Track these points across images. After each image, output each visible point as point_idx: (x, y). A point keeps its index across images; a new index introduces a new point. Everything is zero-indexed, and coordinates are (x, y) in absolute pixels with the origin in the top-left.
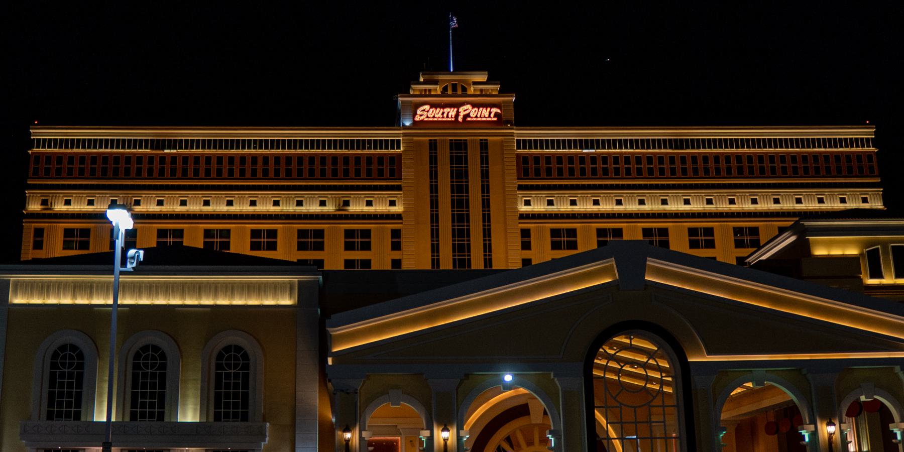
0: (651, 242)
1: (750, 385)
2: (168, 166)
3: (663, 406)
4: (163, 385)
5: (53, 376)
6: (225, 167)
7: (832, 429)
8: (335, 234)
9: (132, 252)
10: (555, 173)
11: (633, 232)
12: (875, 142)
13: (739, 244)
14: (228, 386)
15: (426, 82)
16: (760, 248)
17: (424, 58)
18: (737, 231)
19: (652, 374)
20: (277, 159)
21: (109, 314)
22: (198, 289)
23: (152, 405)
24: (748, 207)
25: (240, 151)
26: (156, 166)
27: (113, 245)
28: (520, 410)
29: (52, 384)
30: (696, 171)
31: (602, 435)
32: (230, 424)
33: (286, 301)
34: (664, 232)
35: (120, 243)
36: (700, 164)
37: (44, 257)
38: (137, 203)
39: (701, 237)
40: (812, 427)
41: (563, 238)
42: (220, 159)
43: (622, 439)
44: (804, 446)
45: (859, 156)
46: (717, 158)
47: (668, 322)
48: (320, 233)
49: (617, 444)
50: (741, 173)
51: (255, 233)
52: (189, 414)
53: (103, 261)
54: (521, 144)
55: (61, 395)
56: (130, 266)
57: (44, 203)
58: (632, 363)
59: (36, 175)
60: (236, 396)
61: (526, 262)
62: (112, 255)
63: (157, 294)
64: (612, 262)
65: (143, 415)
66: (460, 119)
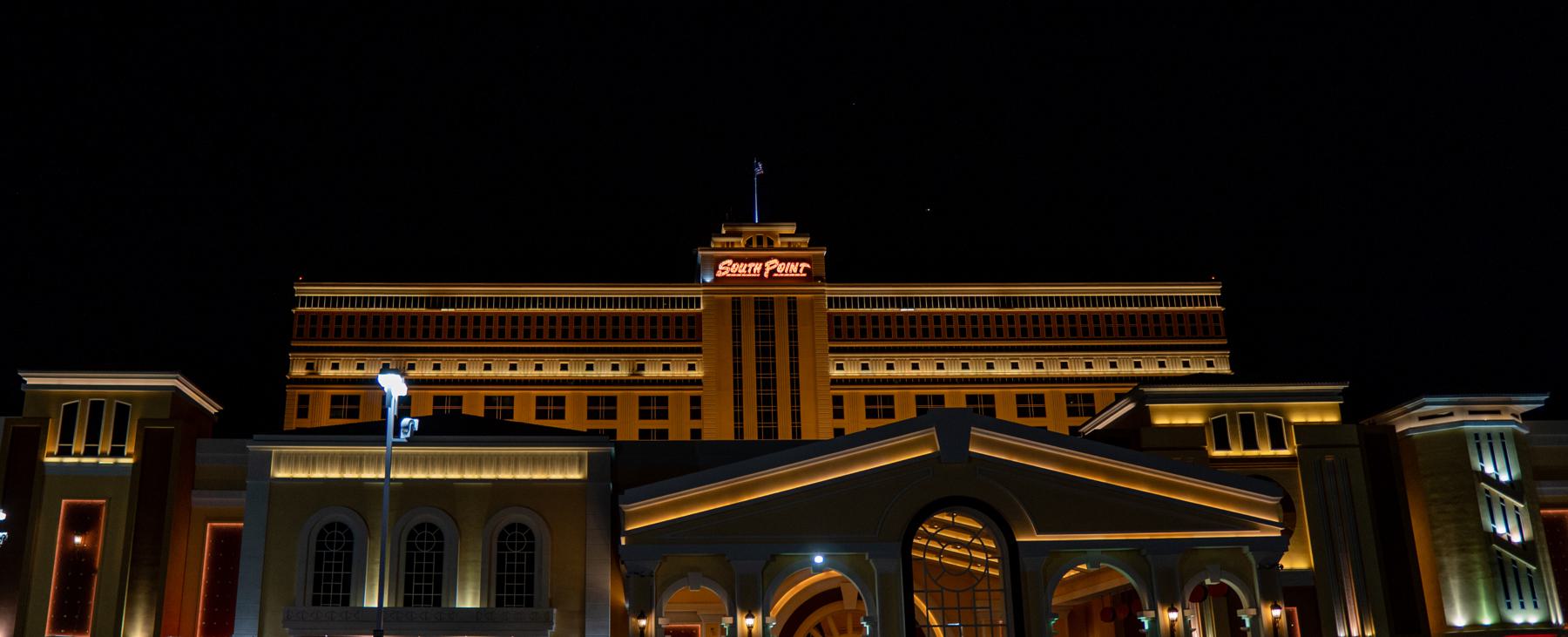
0: (976, 410)
1: (1084, 567)
2: (445, 326)
3: (989, 590)
4: (439, 567)
5: (319, 558)
6: (508, 327)
7: (1174, 615)
8: (628, 403)
9: (405, 421)
10: (882, 334)
11: (955, 399)
12: (1221, 301)
13: (1072, 412)
14: (511, 568)
15: (728, 235)
16: (1095, 416)
17: (730, 209)
18: (1070, 398)
19: (976, 555)
20: (565, 318)
21: (380, 490)
22: (479, 462)
23: (428, 589)
24: (1082, 371)
25: (524, 310)
26: (433, 327)
27: (385, 413)
28: (831, 595)
29: (318, 566)
30: (975, 332)
31: (921, 622)
32: (512, 611)
33: (575, 475)
34: (990, 399)
35: (392, 411)
36: (1029, 324)
37: (309, 426)
38: (412, 367)
39: (1031, 405)
40: (1152, 614)
41: (879, 406)
42: (502, 319)
43: (943, 626)
44: (1144, 635)
45: (1203, 315)
46: (1047, 317)
47: (996, 498)
48: (612, 401)
49: (938, 631)
50: (1074, 334)
51: (541, 401)
52: (468, 599)
53: (374, 431)
54: (834, 302)
55: (328, 578)
56: (403, 437)
57: (309, 367)
58: (955, 543)
59: (301, 337)
60: (520, 579)
61: (839, 432)
62: (384, 424)
63: (433, 467)
64: (932, 432)
65: (418, 601)
66: (766, 275)
